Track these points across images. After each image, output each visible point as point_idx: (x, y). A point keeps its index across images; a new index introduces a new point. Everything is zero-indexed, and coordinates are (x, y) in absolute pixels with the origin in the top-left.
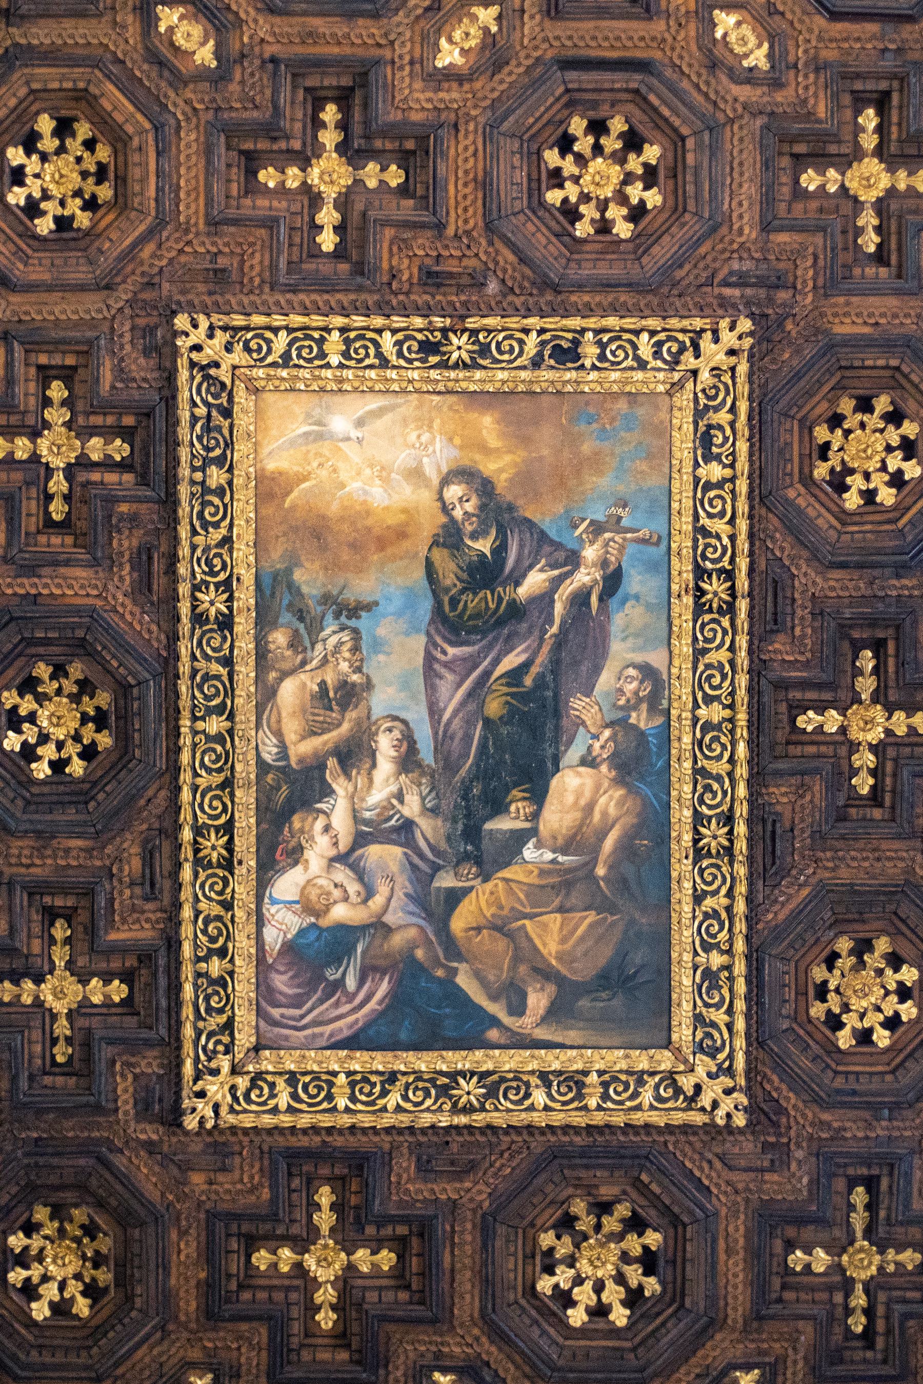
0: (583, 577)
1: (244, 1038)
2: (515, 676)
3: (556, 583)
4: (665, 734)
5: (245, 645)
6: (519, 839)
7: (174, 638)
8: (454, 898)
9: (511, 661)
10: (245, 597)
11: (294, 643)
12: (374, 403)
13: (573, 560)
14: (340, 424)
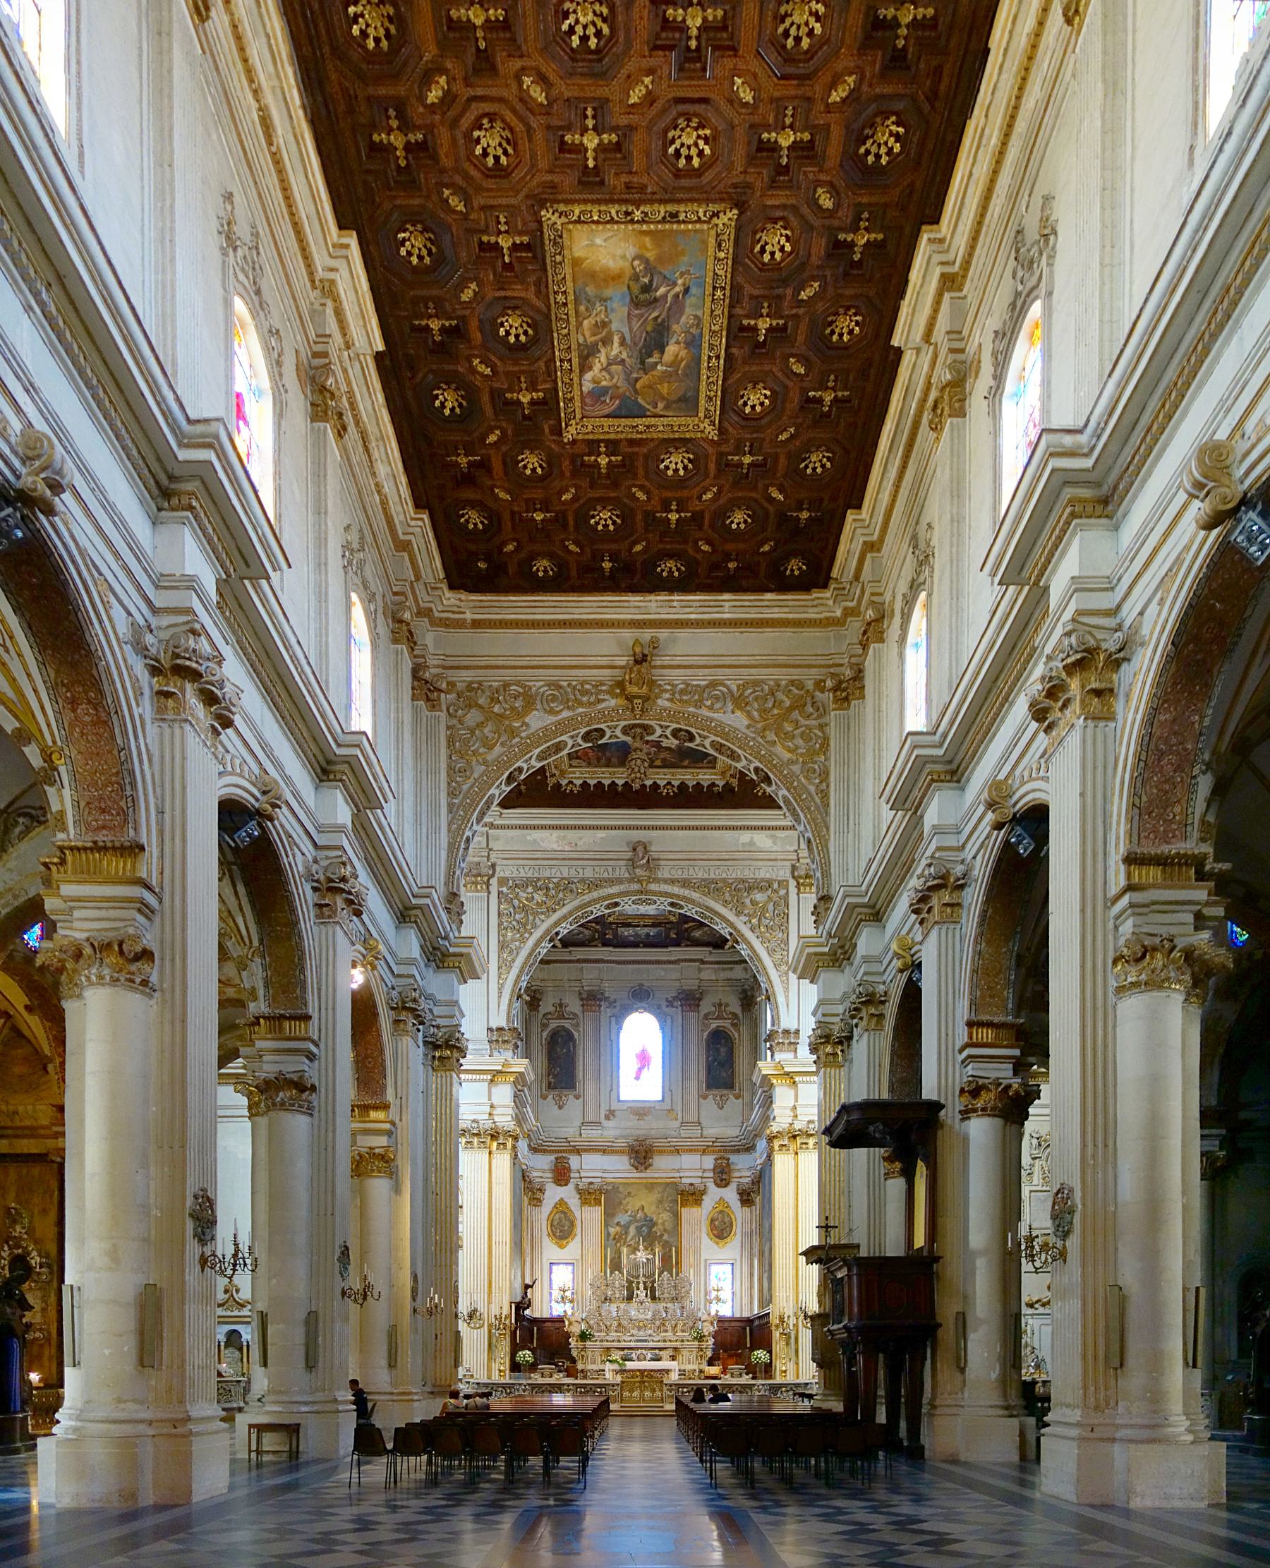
0: (677, 289)
1: (578, 416)
2: (656, 318)
3: (668, 291)
4: (701, 335)
5: (572, 313)
6: (656, 364)
7: (549, 310)
8: (637, 380)
9: (655, 314)
10: (571, 298)
11: (587, 309)
12: (610, 234)
13: (675, 284)
14: (598, 241)
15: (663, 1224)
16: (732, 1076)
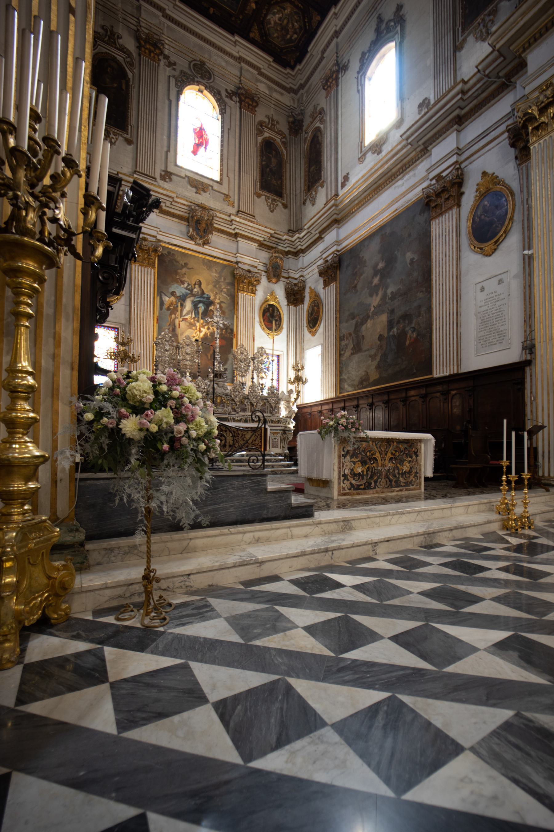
15: (219, 304)
16: (281, 186)
